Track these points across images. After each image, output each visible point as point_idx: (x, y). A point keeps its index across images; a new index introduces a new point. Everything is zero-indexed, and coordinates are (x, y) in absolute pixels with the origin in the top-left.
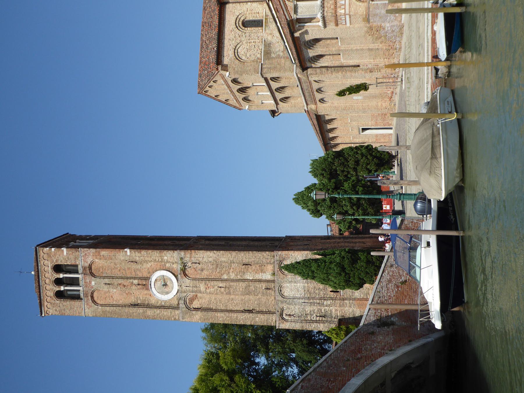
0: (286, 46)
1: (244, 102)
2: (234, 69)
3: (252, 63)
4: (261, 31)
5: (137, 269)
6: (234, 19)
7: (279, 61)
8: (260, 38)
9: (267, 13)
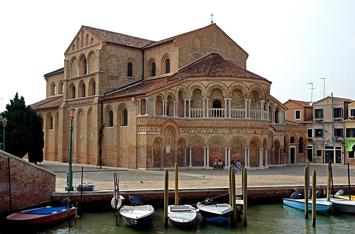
0: (116, 90)
1: (72, 57)
2: (103, 54)
3: (106, 66)
4: (126, 75)
6: (134, 57)
7: (107, 85)
8: (121, 73)
9: (135, 80)
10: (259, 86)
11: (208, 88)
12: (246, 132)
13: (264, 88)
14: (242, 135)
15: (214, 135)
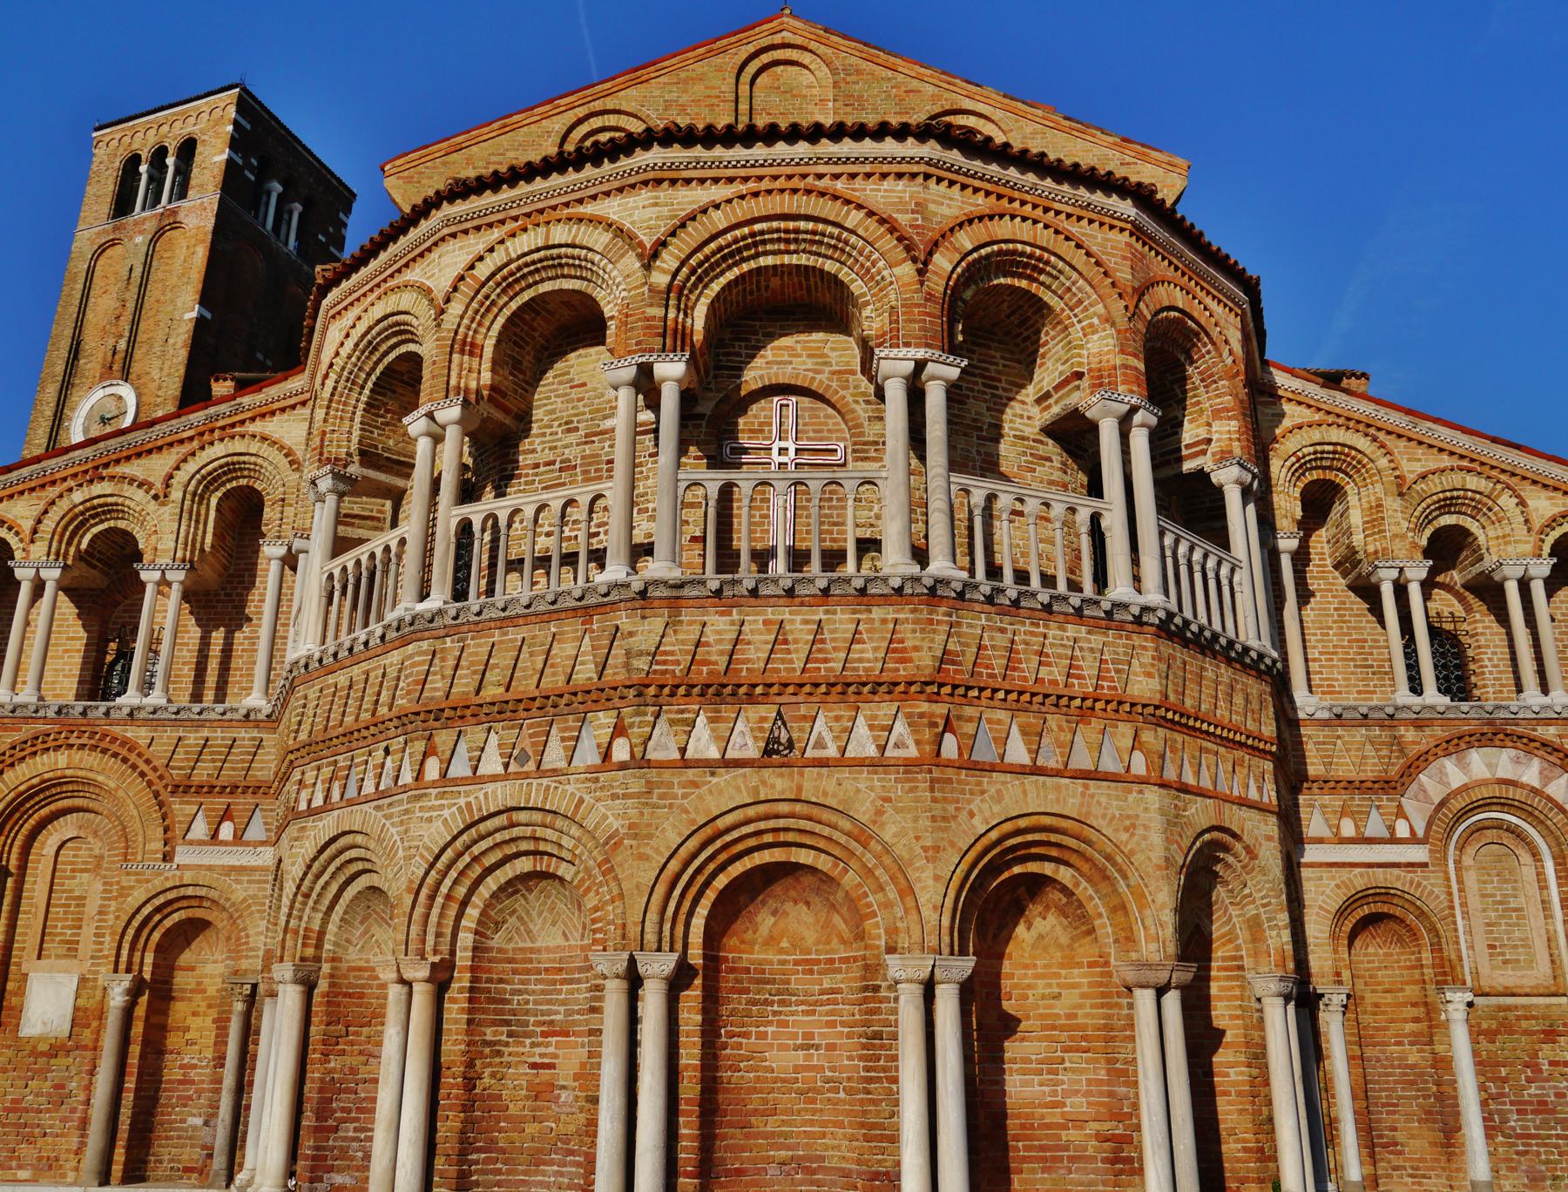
5: (152, 346)
10: (827, 209)
11: (330, 383)
12: (621, 752)
13: (903, 219)
14: (563, 796)
15: (326, 827)
